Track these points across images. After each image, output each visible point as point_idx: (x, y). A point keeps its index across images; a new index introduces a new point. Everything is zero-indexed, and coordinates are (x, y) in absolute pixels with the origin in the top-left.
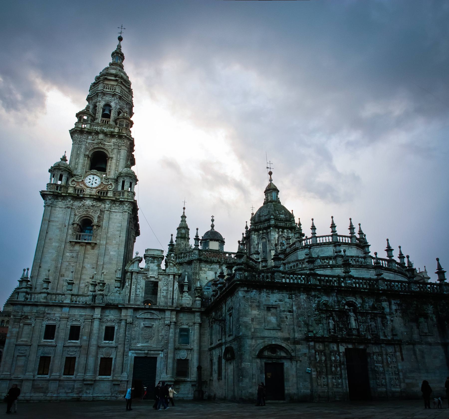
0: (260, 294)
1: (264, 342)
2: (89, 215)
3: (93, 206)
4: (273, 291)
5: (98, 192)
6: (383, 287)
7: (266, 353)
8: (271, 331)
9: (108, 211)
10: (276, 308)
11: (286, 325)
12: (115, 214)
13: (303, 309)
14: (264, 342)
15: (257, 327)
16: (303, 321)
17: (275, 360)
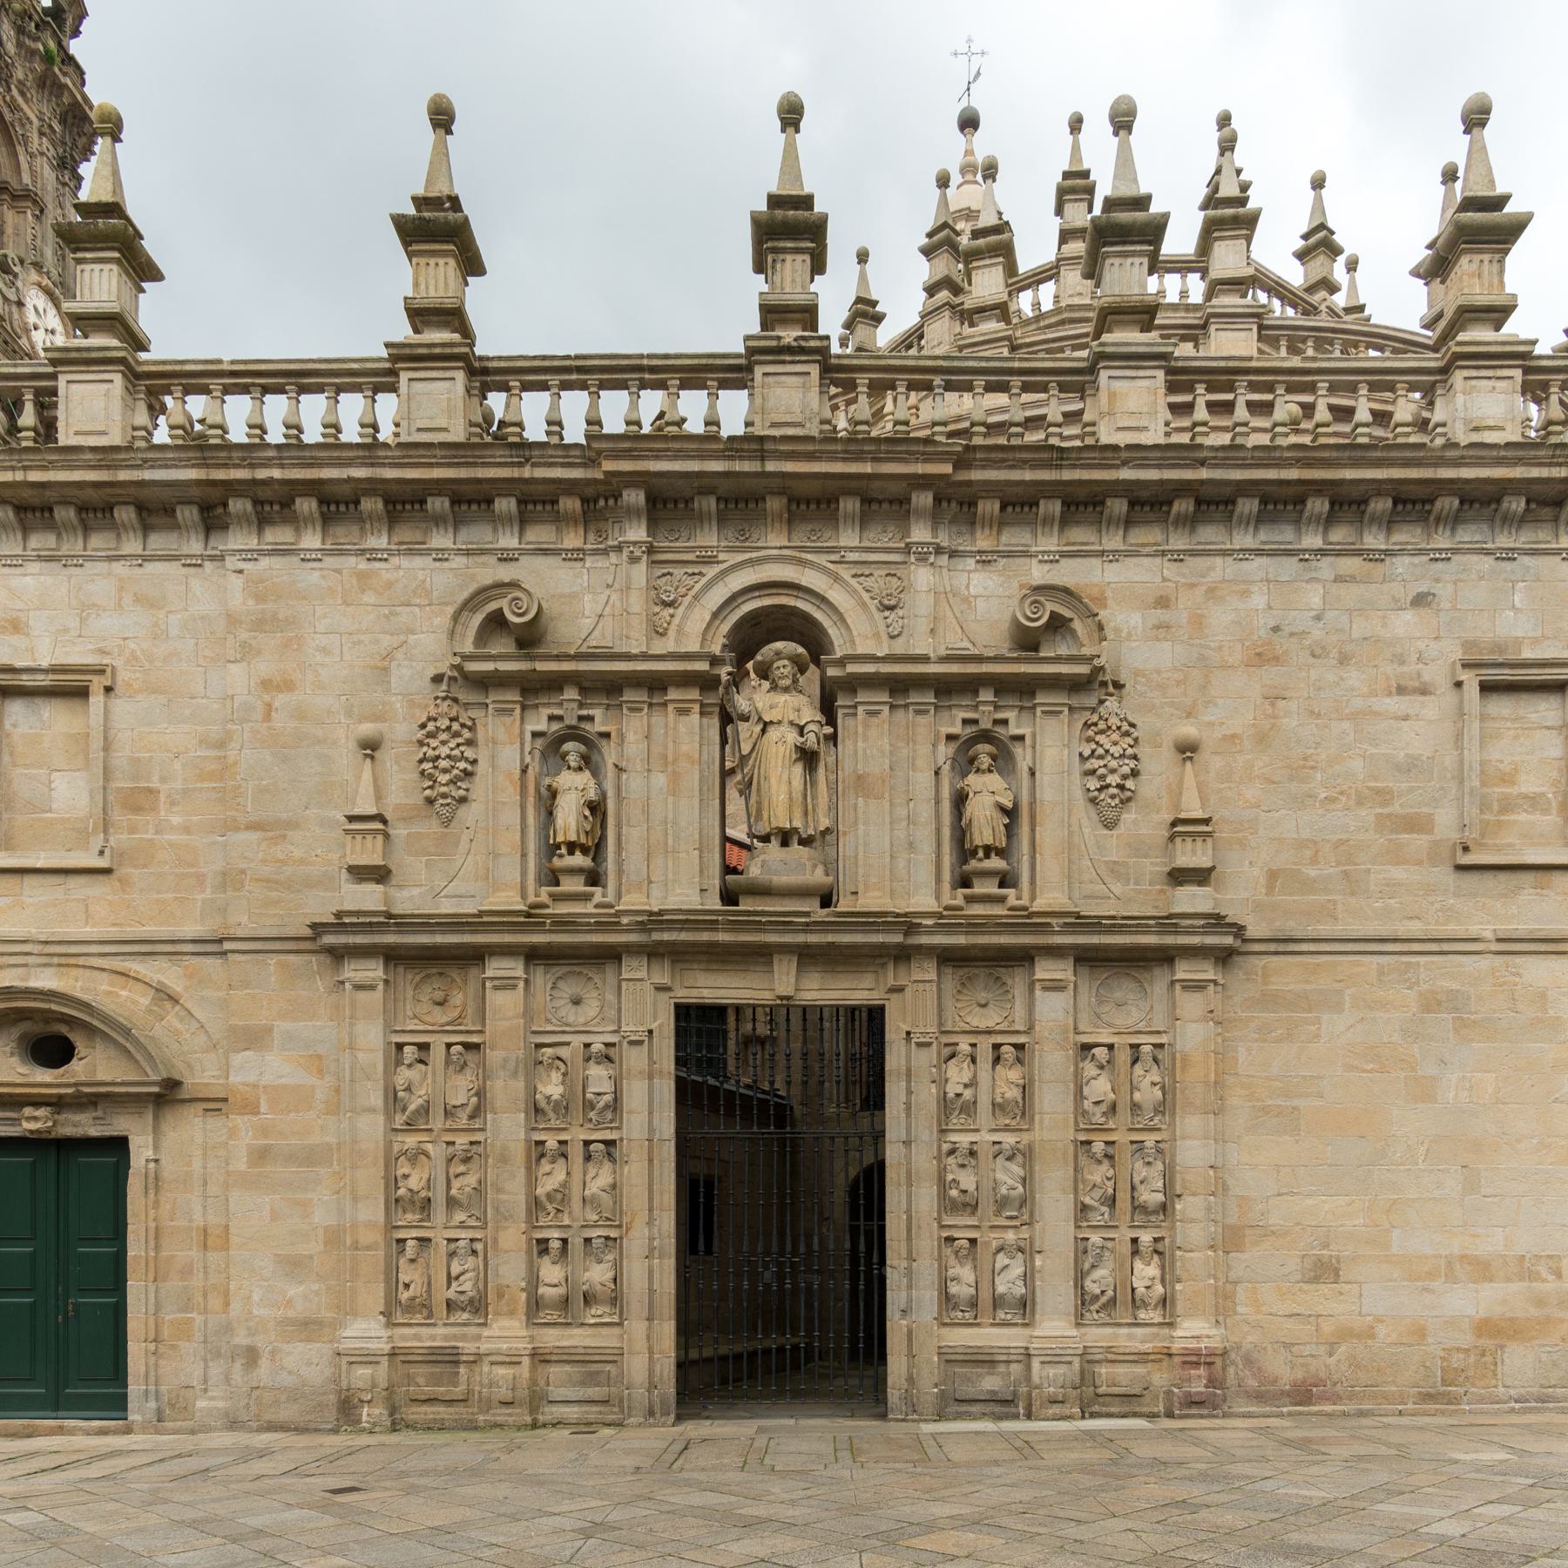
17: (35, 1119)
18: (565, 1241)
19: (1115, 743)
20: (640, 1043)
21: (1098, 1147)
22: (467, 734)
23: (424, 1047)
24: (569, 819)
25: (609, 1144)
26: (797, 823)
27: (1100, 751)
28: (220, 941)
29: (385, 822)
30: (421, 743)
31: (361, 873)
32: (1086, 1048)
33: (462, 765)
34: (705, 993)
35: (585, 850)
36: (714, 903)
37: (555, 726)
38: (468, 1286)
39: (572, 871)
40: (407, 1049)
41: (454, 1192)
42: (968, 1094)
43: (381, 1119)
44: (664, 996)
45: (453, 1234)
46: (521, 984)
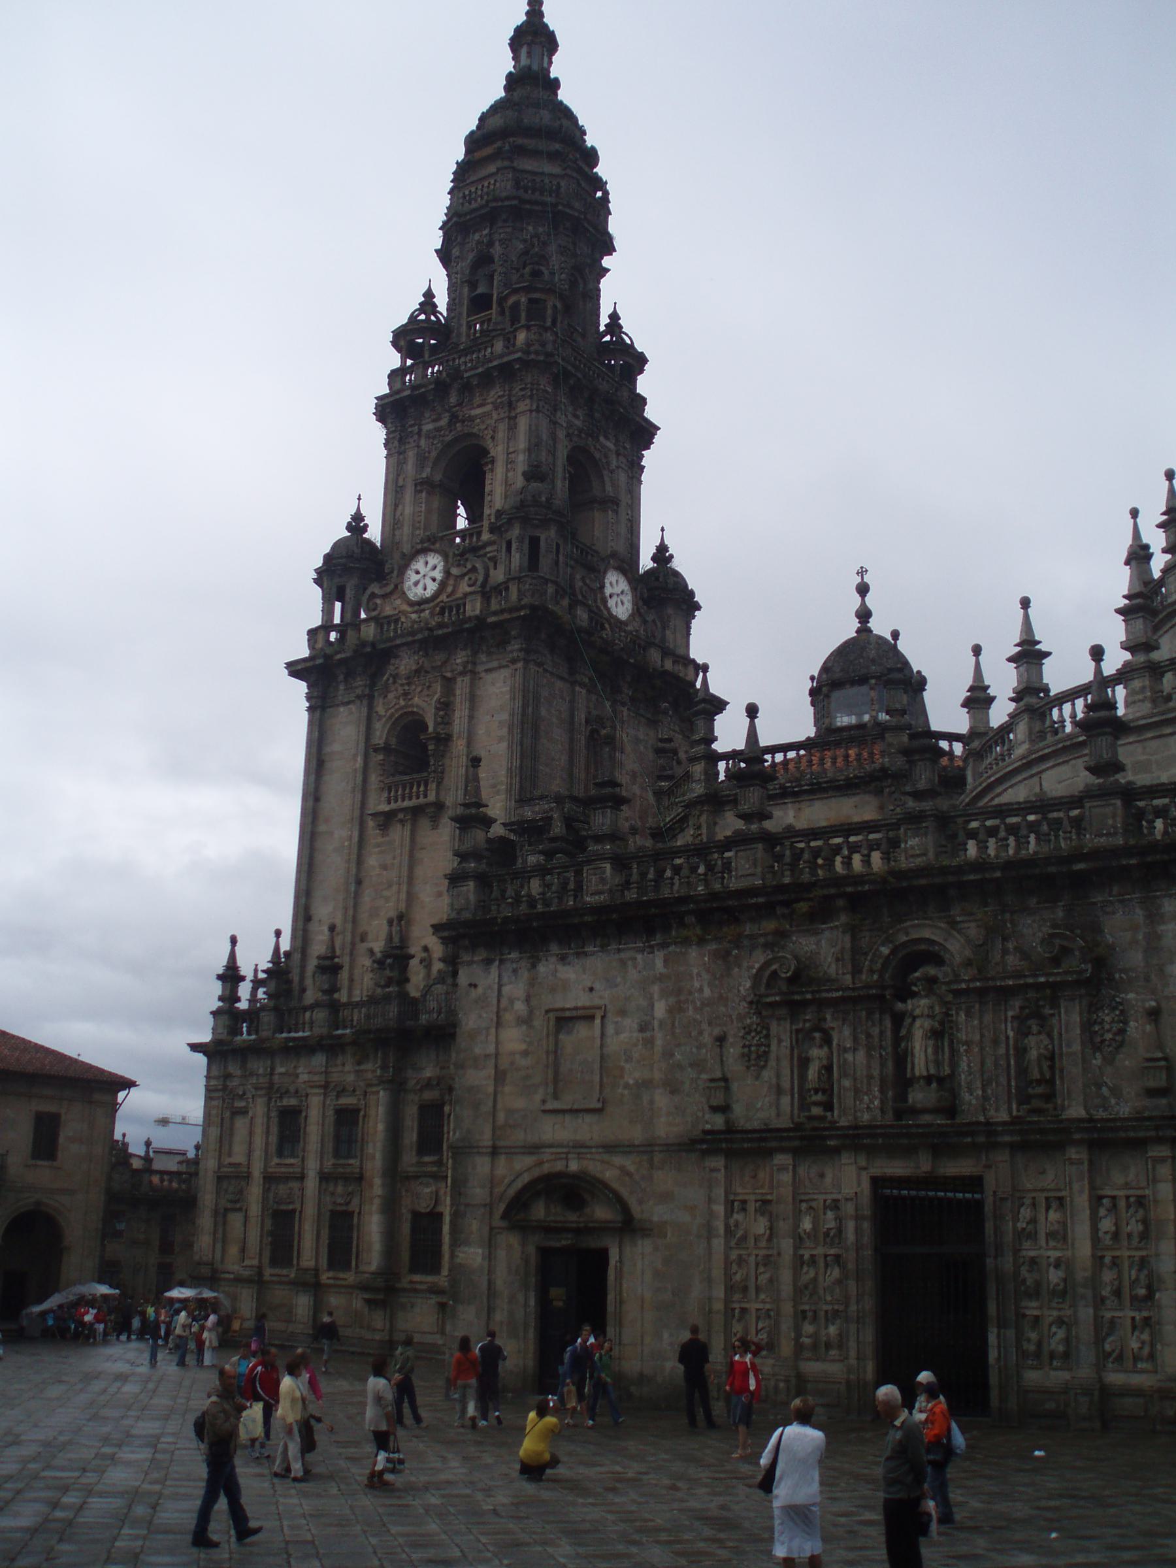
0: (534, 966)
1: (540, 1163)
2: (412, 706)
3: (417, 672)
4: (583, 947)
5: (442, 613)
6: (1108, 835)
7: (539, 1211)
8: (568, 1117)
9: (462, 674)
10: (592, 1018)
11: (627, 1086)
12: (489, 677)
13: (696, 1009)
14: (540, 1163)
15: (519, 1103)
16: (691, 1065)
18: (815, 1312)
19: (1108, 1015)
20: (851, 1199)
21: (1107, 1260)
22: (765, 1032)
23: (744, 1202)
24: (812, 1073)
25: (837, 1257)
26: (932, 1071)
27: (1099, 1020)
28: (650, 1145)
29: (725, 1079)
30: (743, 1038)
31: (715, 1109)
32: (1100, 1198)
33: (763, 1049)
34: (886, 1170)
35: (824, 1091)
36: (889, 1118)
37: (807, 1025)
38: (765, 1336)
39: (816, 1104)
40: (736, 1204)
41: (759, 1282)
42: (1030, 1227)
43: (722, 1241)
44: (864, 1173)
45: (760, 1306)
46: (791, 1167)
